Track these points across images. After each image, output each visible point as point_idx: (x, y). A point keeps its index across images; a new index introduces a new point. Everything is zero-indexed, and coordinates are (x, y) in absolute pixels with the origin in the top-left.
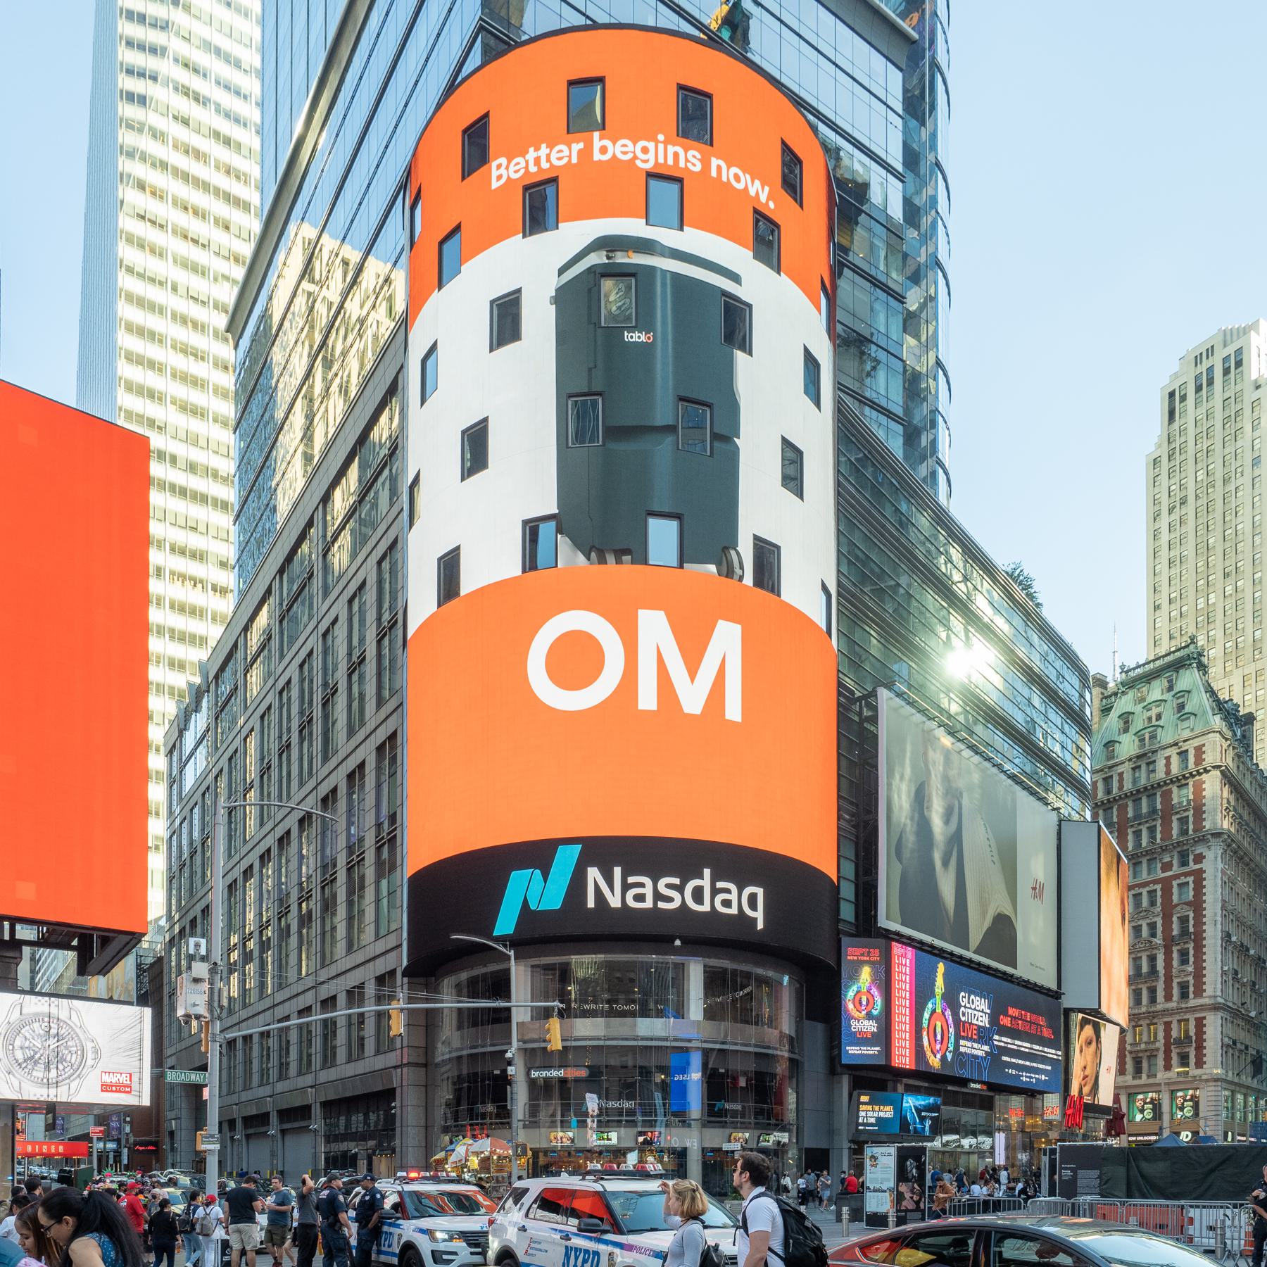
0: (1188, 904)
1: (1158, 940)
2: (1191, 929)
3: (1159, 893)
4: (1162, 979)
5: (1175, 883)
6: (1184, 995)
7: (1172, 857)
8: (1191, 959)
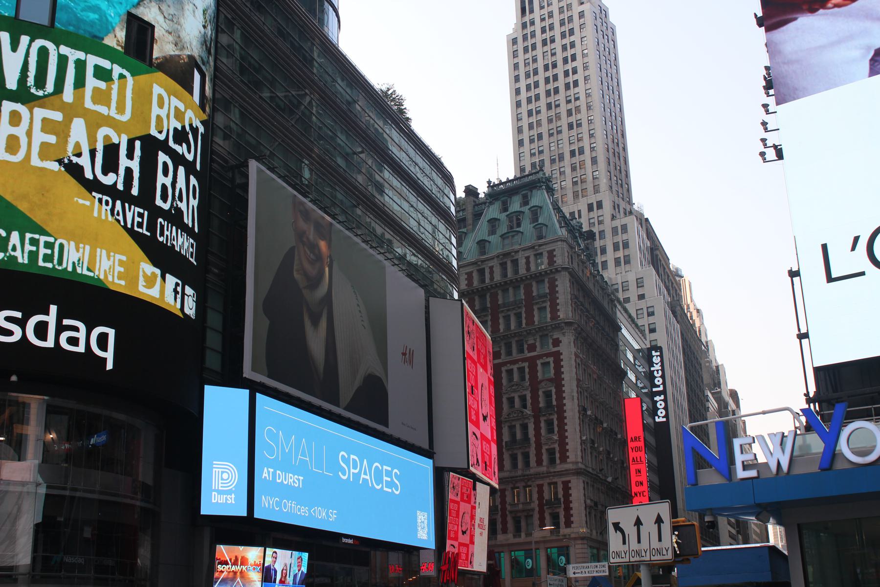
0: (550, 380)
1: (528, 411)
2: (554, 403)
3: (527, 370)
4: (533, 445)
5: (539, 362)
6: (552, 461)
7: (535, 340)
8: (556, 429)
